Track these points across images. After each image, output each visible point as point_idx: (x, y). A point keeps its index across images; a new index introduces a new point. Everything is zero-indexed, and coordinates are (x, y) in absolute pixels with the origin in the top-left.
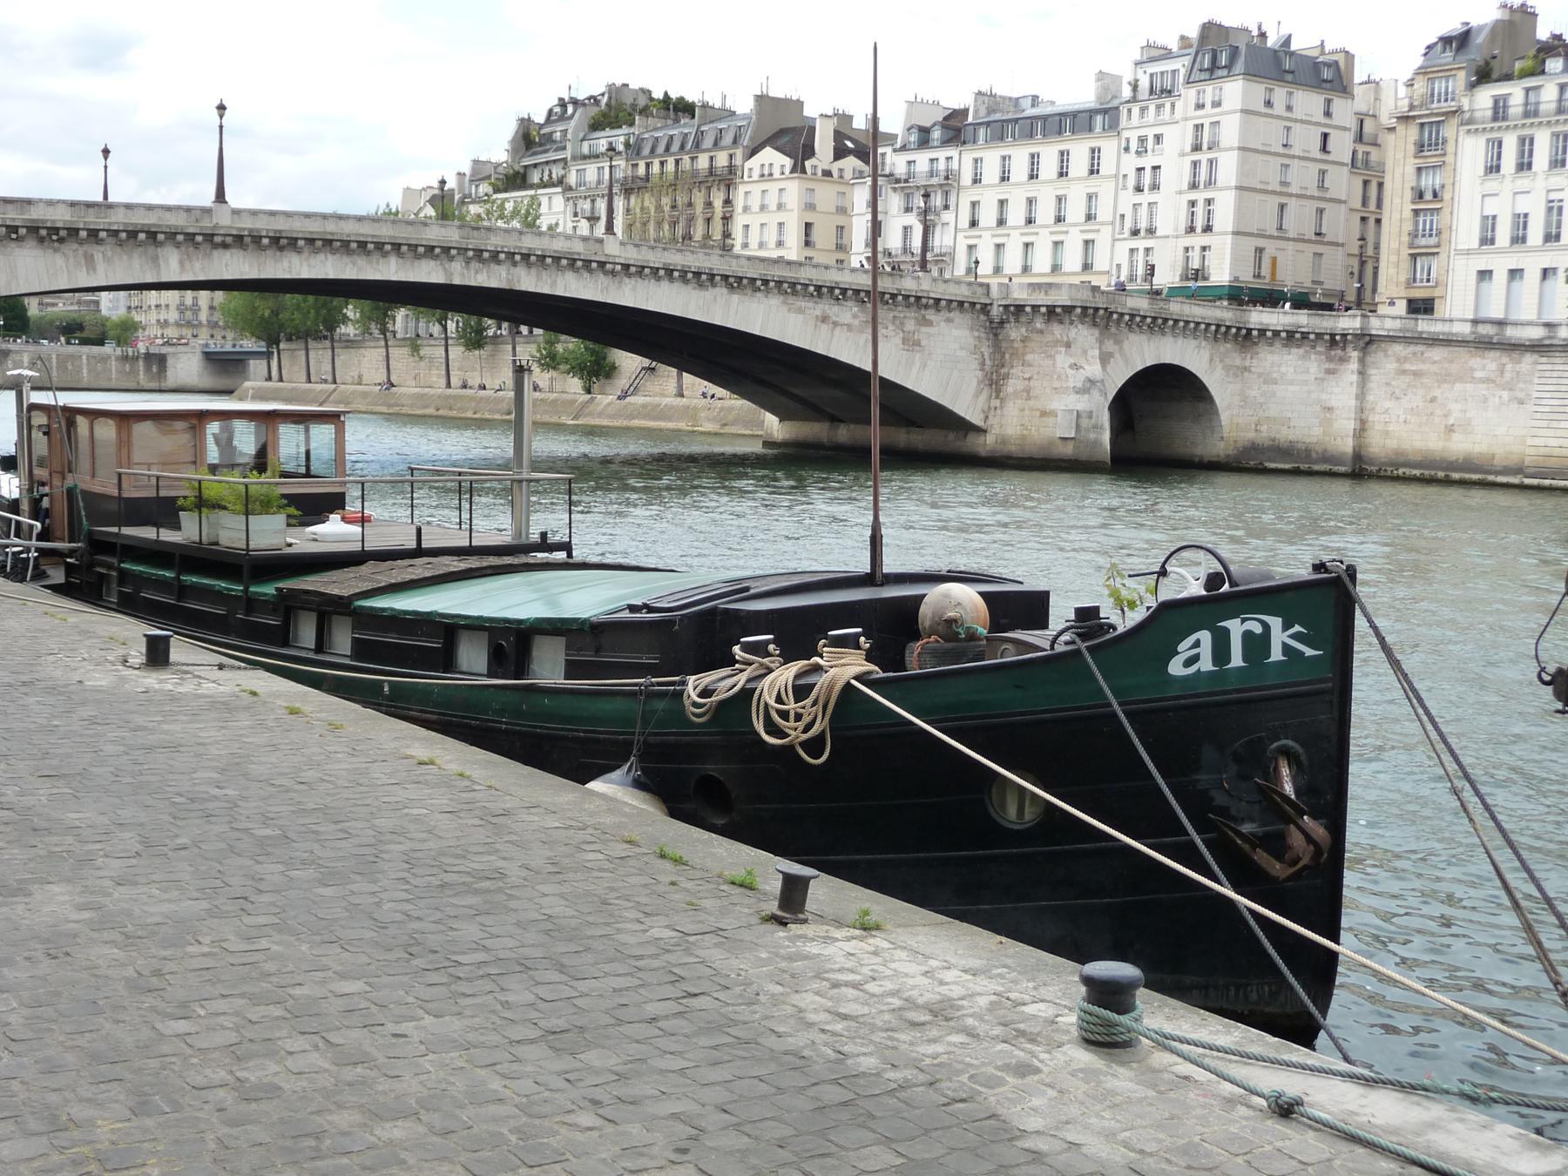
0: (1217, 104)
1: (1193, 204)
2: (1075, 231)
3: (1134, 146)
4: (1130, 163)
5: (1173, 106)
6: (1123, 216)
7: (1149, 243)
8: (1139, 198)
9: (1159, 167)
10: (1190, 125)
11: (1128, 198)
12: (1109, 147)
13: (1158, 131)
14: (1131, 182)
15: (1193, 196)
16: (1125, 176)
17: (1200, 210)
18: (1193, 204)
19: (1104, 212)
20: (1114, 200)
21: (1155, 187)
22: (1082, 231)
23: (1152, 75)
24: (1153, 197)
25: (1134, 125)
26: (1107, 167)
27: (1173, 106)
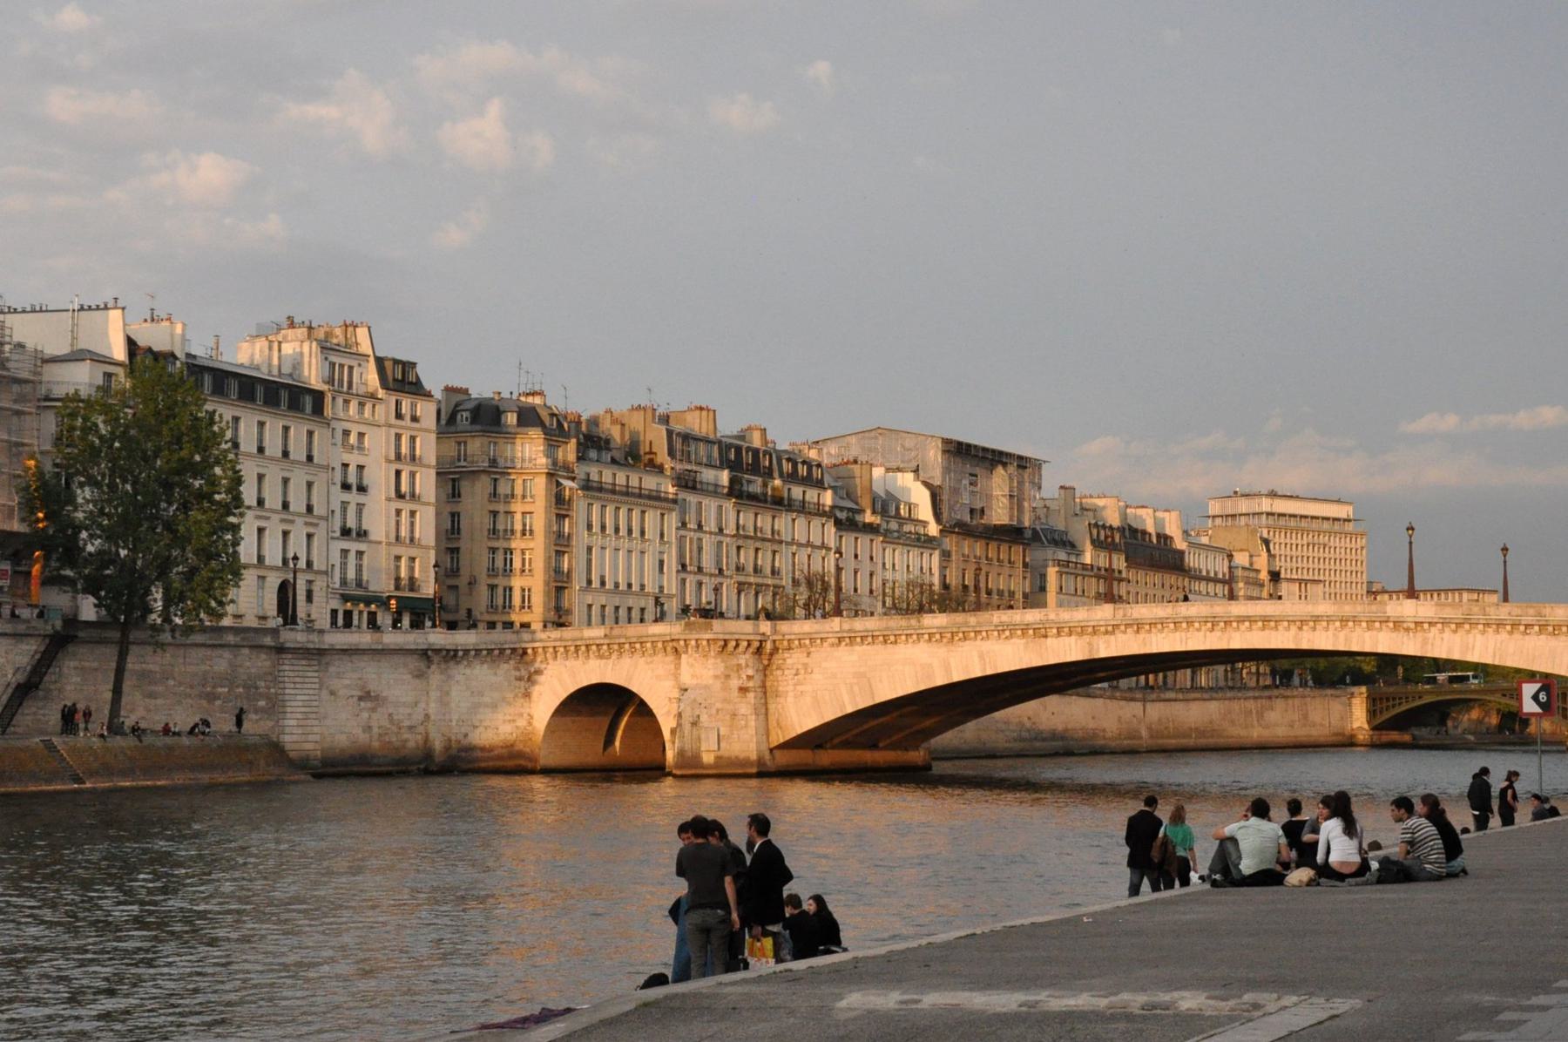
1: (398, 512)
2: (300, 521)
8: (346, 497)
10: (393, 431)
11: (338, 496)
13: (362, 429)
15: (400, 504)
18: (398, 512)
20: (328, 497)
22: (306, 524)
24: (361, 499)
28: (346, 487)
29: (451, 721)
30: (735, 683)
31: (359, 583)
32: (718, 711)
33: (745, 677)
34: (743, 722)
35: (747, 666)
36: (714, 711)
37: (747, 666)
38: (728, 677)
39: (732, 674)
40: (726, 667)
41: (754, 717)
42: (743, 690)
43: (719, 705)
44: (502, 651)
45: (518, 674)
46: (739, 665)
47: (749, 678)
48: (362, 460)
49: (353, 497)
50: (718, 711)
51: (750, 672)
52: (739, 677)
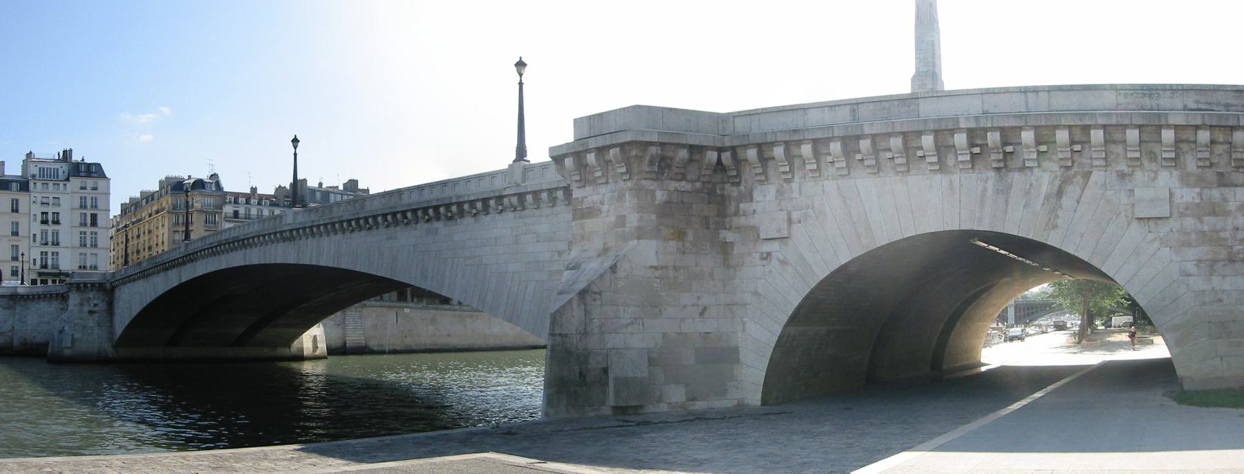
0: (95, 189)
3: (39, 200)
4: (37, 210)
5: (65, 185)
6: (34, 235)
7: (55, 249)
8: (45, 227)
9: (58, 213)
11: (37, 228)
12: (23, 199)
14: (39, 218)
16: (35, 215)
17: (88, 236)
19: (22, 231)
21: (57, 222)
22: (10, 240)
23: (40, 168)
24: (56, 227)
25: (37, 190)
26: (23, 207)
27: (65, 185)
28: (45, 222)
29: (27, 330)
30: (86, 309)
31: (55, 266)
32: (75, 324)
33: (92, 305)
34: (90, 331)
35: (94, 298)
36: (73, 324)
37: (94, 298)
38: (82, 305)
39: (85, 303)
40: (81, 299)
41: (97, 328)
42: (91, 312)
43: (76, 321)
44: (51, 295)
45: (61, 306)
46: (89, 298)
47: (95, 305)
48: (56, 210)
49: (51, 228)
50: (75, 324)
51: (96, 302)
52: (89, 305)
